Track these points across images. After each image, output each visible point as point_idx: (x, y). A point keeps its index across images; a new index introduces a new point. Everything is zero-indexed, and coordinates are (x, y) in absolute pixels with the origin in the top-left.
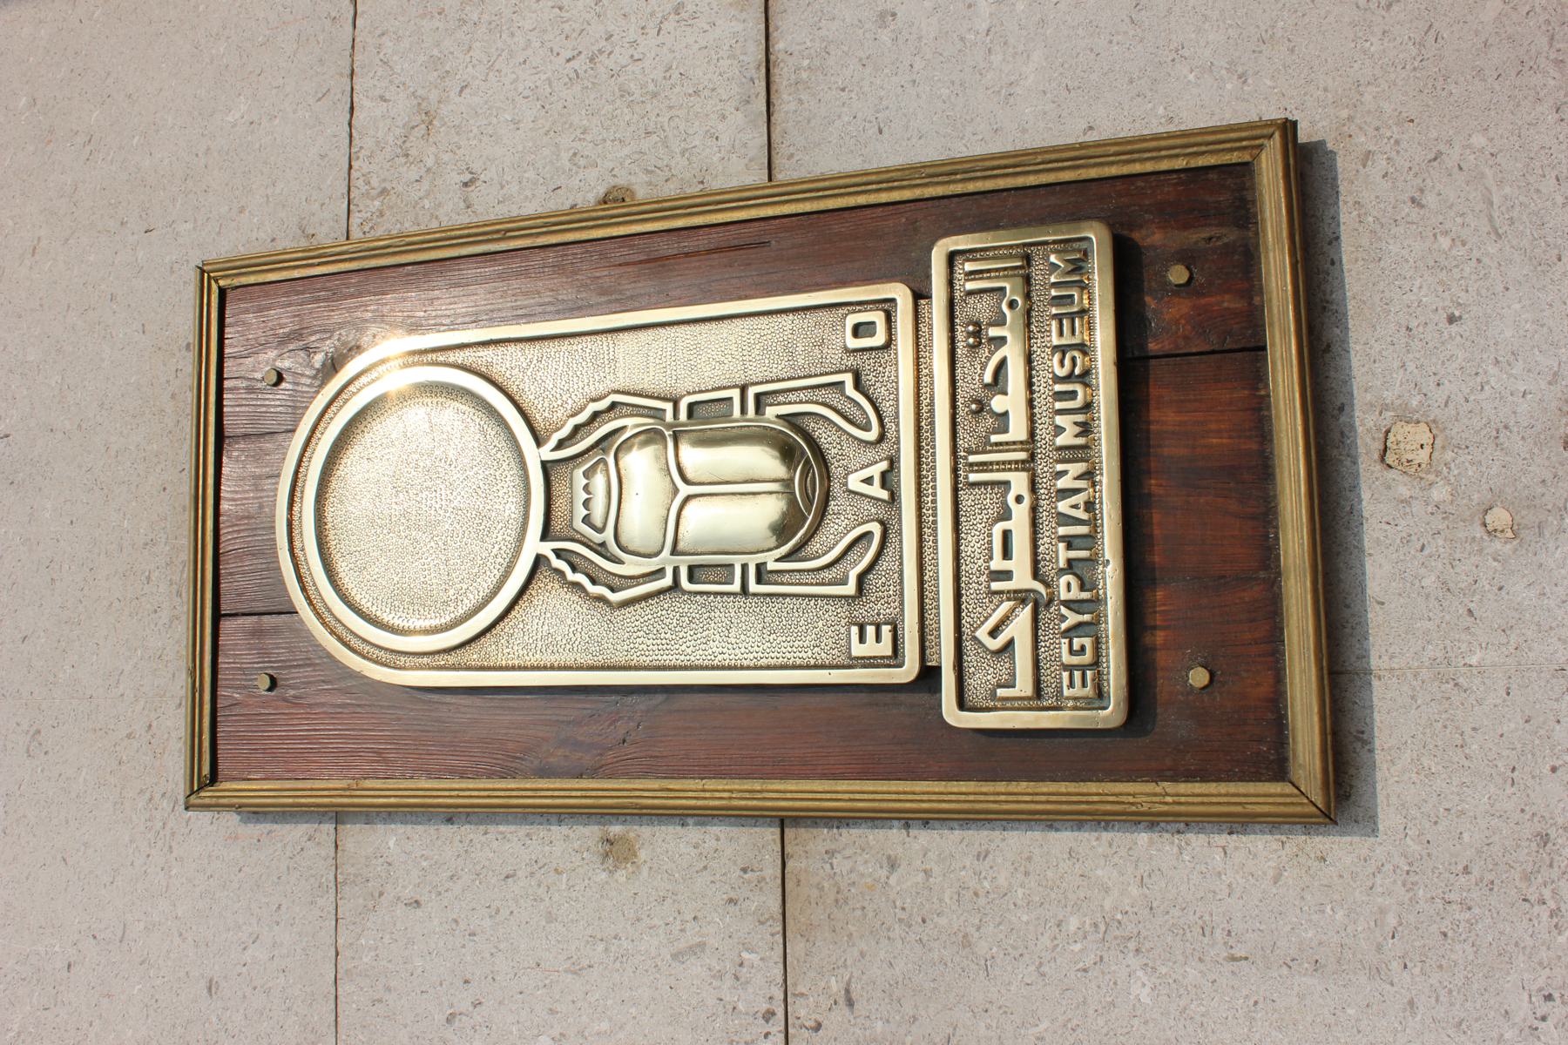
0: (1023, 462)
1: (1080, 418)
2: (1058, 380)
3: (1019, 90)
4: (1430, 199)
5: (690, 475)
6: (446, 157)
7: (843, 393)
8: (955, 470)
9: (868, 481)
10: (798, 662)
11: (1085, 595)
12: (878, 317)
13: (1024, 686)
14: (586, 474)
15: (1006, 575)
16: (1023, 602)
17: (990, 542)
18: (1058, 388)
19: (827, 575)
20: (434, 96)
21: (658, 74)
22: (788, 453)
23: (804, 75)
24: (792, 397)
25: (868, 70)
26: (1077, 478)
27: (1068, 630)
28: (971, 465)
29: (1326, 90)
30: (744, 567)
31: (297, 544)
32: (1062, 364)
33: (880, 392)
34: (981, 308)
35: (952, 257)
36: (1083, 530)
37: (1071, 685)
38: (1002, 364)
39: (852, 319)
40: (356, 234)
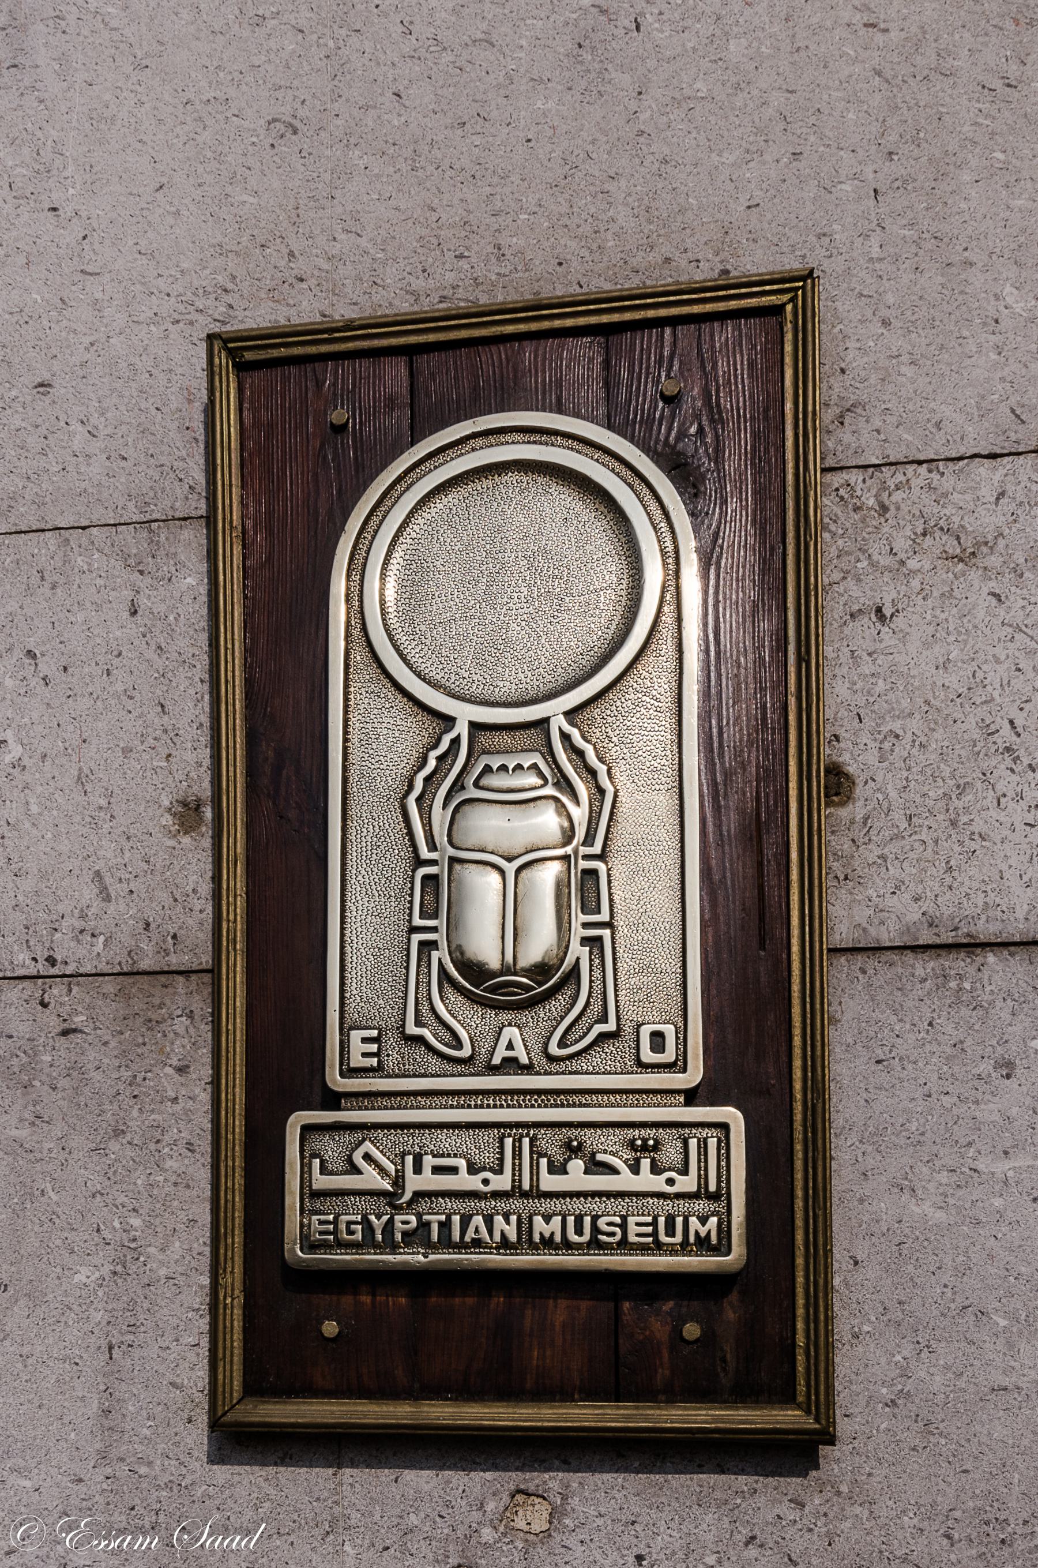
0: (520, 1186)
1: (558, 1238)
2: (595, 1219)
3: (906, 1197)
4: (752, 1552)
5: (524, 874)
6: (915, 583)
7: (597, 1022)
8: (518, 1125)
9: (510, 1046)
10: (347, 982)
11: (398, 1237)
12: (669, 1055)
13: (321, 1181)
14: (534, 767)
15: (418, 1169)
16: (395, 1184)
17: (449, 1156)
18: (587, 1220)
19: (425, 1009)
20: (994, 561)
21: (978, 826)
22: (541, 970)
23: (953, 984)
24: (597, 973)
25: (949, 1050)
26: (503, 1234)
27: (369, 1222)
28: (520, 1141)
29: (870, 1475)
30: (435, 929)
31: (480, 442)
32: (609, 1224)
33: (596, 1058)
34: (671, 1153)
35: (724, 1127)
36: (456, 1236)
37: (321, 1222)
38: (615, 1171)
39: (669, 1030)
40: (836, 479)
